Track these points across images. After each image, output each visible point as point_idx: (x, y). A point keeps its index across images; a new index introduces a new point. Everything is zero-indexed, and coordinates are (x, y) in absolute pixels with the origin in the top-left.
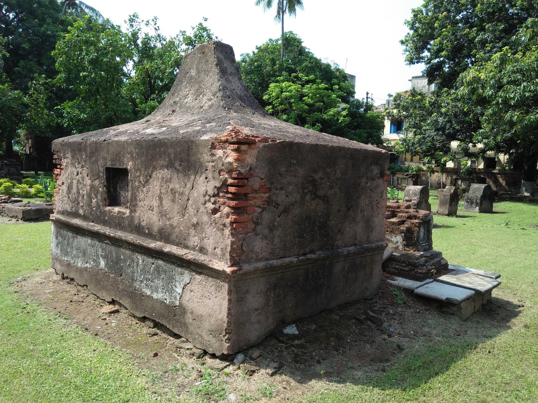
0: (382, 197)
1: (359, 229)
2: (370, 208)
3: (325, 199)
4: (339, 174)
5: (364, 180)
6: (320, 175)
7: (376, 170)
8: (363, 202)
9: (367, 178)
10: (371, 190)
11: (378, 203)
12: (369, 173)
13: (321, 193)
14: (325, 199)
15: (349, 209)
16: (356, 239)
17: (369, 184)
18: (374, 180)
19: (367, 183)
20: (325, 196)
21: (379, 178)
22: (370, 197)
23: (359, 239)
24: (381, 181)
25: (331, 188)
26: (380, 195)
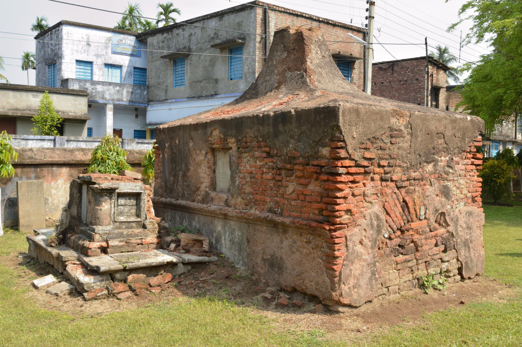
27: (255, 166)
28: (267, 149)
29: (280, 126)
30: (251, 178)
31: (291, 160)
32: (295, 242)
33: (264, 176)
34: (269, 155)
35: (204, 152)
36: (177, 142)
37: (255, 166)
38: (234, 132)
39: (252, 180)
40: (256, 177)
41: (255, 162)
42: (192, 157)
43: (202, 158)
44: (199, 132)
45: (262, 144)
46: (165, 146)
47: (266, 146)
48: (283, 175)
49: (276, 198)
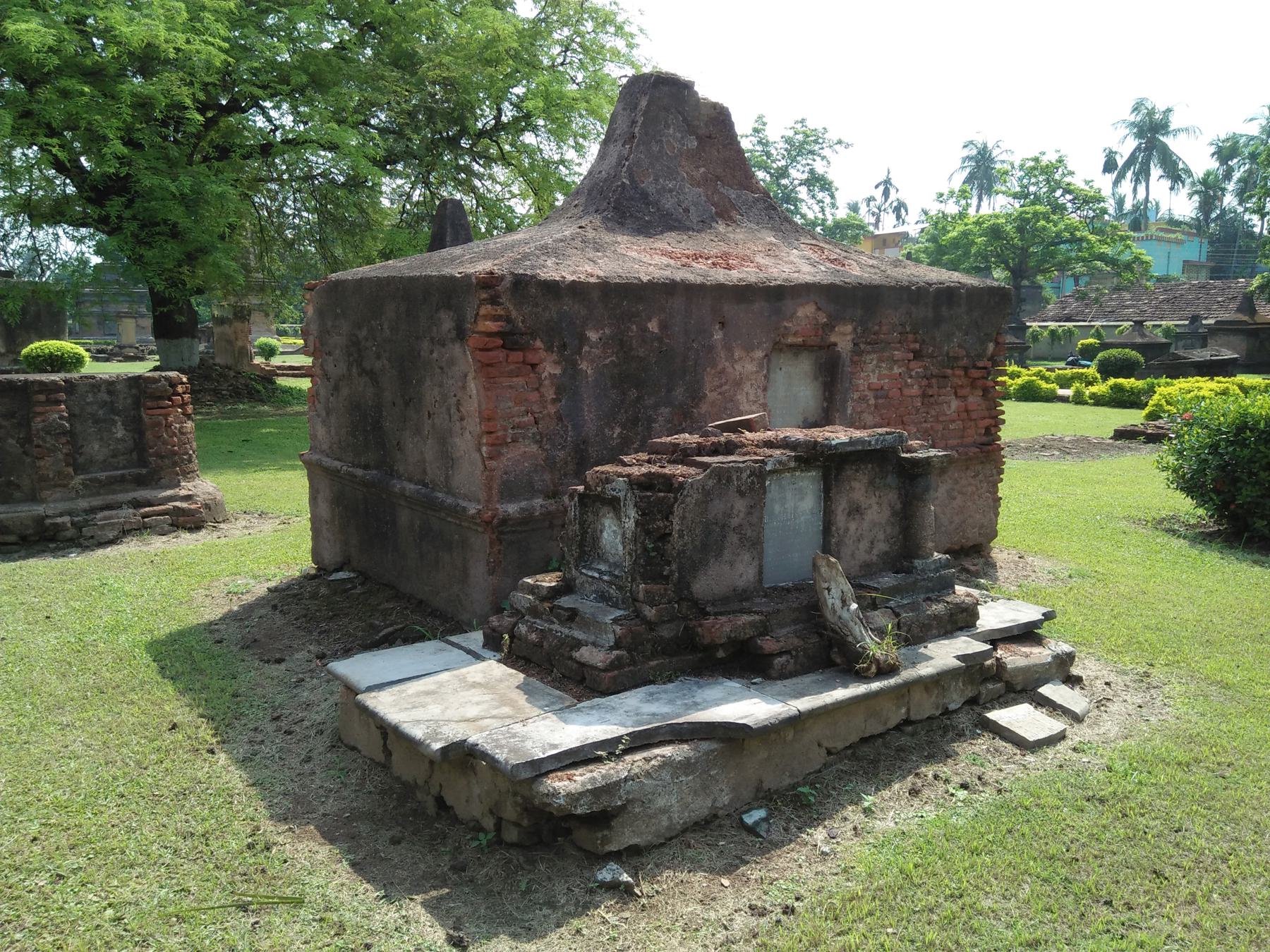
0: (464, 388)
1: (430, 451)
2: (444, 409)
3: (372, 375)
4: (387, 332)
5: (425, 345)
6: (364, 332)
7: (447, 323)
8: (431, 394)
9: (432, 339)
10: (441, 368)
11: (458, 404)
12: (435, 329)
13: (367, 365)
14: (372, 375)
15: (407, 404)
16: (424, 472)
17: (435, 355)
18: (444, 345)
19: (432, 352)
20: (371, 370)
21: (453, 341)
22: (441, 386)
23: (429, 471)
24: (456, 349)
25: (378, 357)
26: (460, 384)
27: (890, 377)
28: (917, 346)
29: (944, 309)
30: (876, 398)
31: (952, 361)
32: (956, 482)
33: (906, 391)
34: (918, 355)
35: (759, 354)
36: (653, 326)
37: (890, 377)
38: (860, 312)
39: (880, 401)
40: (891, 394)
41: (891, 369)
42: (714, 366)
43: (750, 367)
44: (756, 306)
45: (911, 336)
46: (583, 339)
47: (916, 341)
48: (935, 386)
49: (925, 425)
